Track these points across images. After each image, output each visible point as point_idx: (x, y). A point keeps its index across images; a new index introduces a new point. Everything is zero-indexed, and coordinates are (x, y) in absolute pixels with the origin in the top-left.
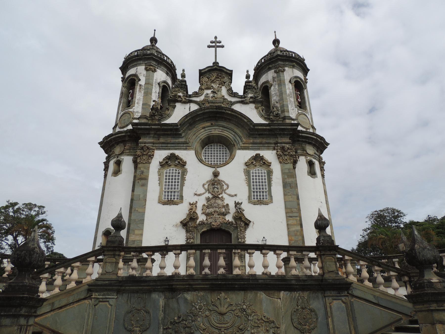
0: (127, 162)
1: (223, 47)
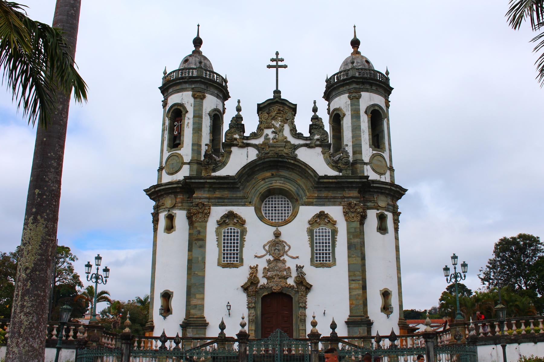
0: (181, 216)
1: (285, 67)
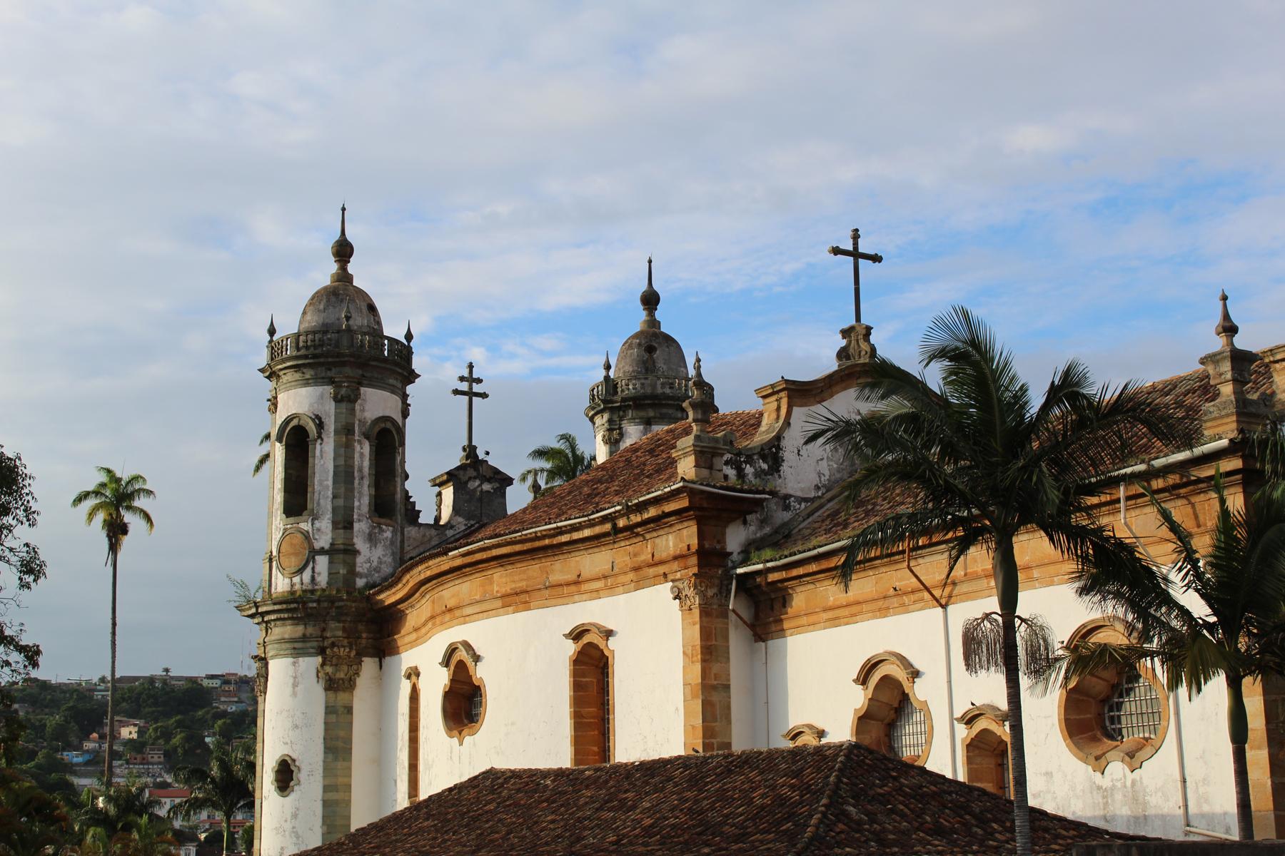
1: (484, 396)
